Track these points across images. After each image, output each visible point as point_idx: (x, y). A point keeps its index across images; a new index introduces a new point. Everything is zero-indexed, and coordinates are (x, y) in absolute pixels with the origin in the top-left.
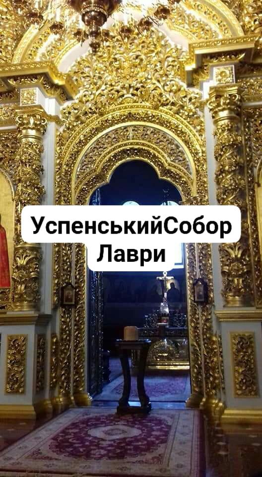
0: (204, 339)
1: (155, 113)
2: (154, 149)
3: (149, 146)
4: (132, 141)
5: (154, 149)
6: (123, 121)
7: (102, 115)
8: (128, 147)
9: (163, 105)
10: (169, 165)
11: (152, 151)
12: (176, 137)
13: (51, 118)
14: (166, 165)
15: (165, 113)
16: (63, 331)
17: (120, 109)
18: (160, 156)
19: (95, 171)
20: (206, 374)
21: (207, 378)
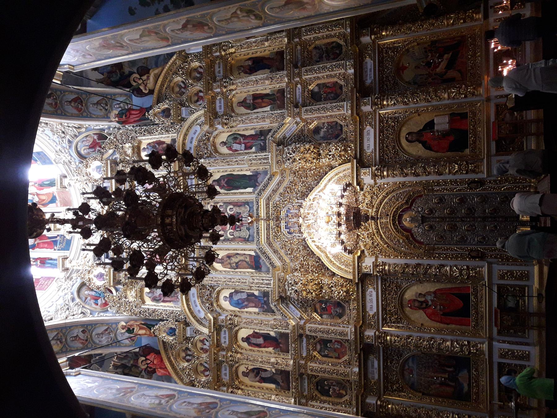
0: (500, 184)
1: (375, 206)
2: (394, 208)
3: (392, 211)
4: (388, 220)
5: (394, 208)
6: (377, 223)
7: (374, 235)
8: (391, 222)
9: (372, 203)
10: (403, 200)
11: (394, 210)
12: (388, 197)
13: (376, 260)
14: (403, 202)
15: (376, 202)
16: (496, 257)
17: (372, 225)
18: (398, 206)
19: (404, 240)
20: (519, 183)
21: (521, 183)
